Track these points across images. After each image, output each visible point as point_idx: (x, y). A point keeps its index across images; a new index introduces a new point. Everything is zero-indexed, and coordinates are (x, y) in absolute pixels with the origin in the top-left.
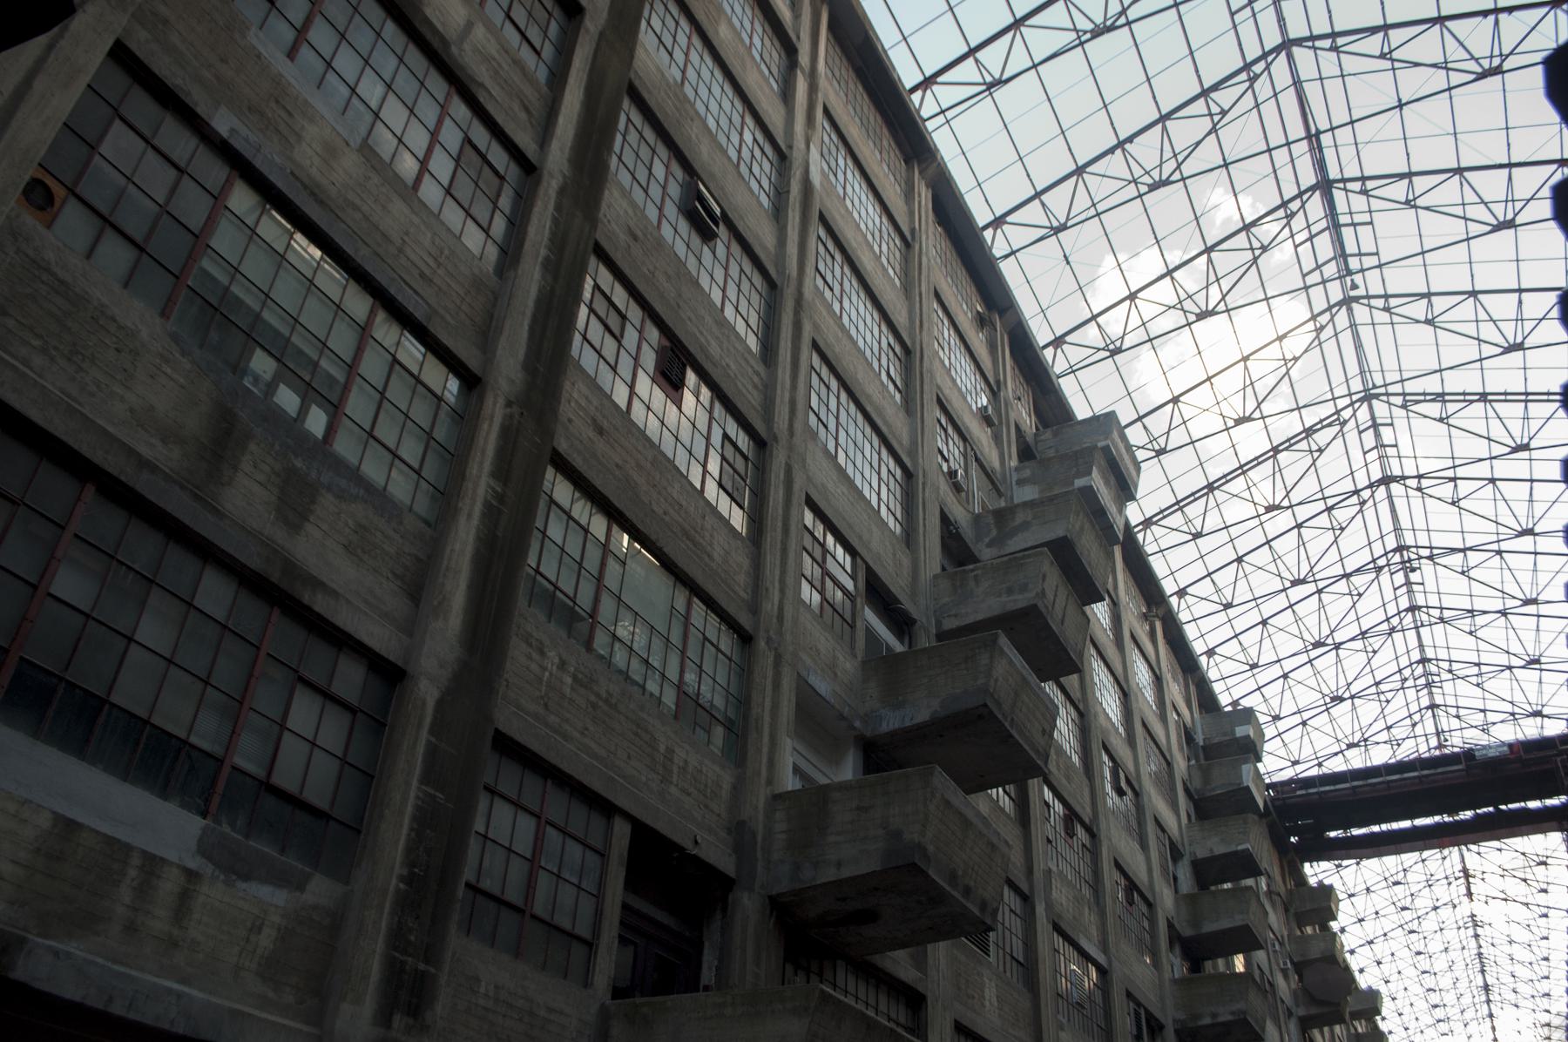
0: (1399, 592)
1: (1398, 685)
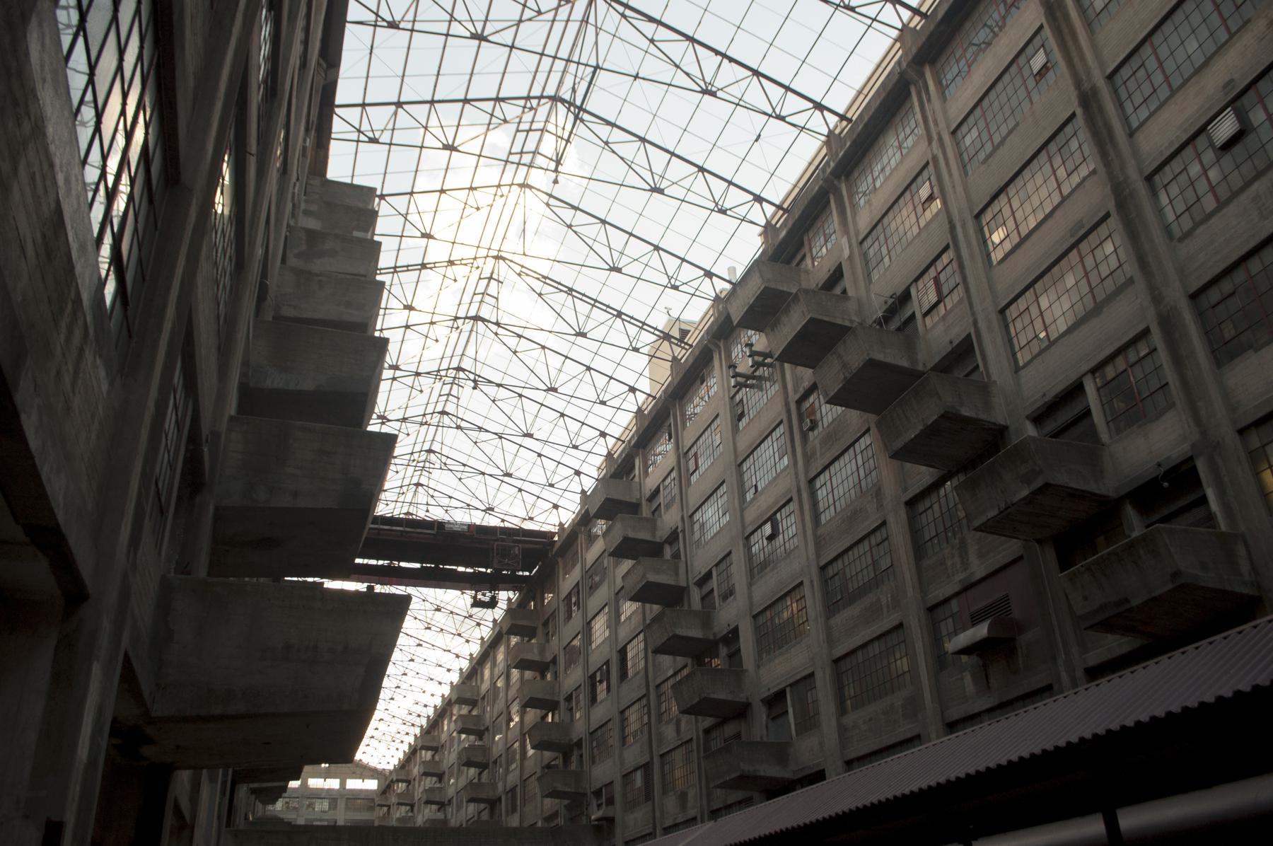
0: (441, 398)
1: (406, 462)
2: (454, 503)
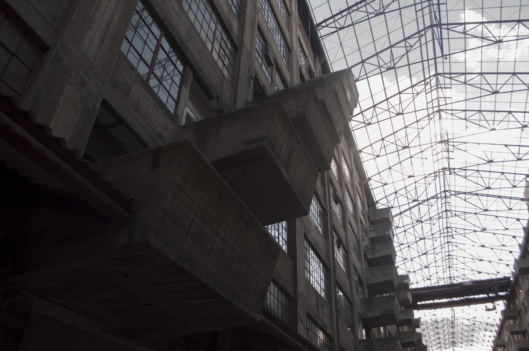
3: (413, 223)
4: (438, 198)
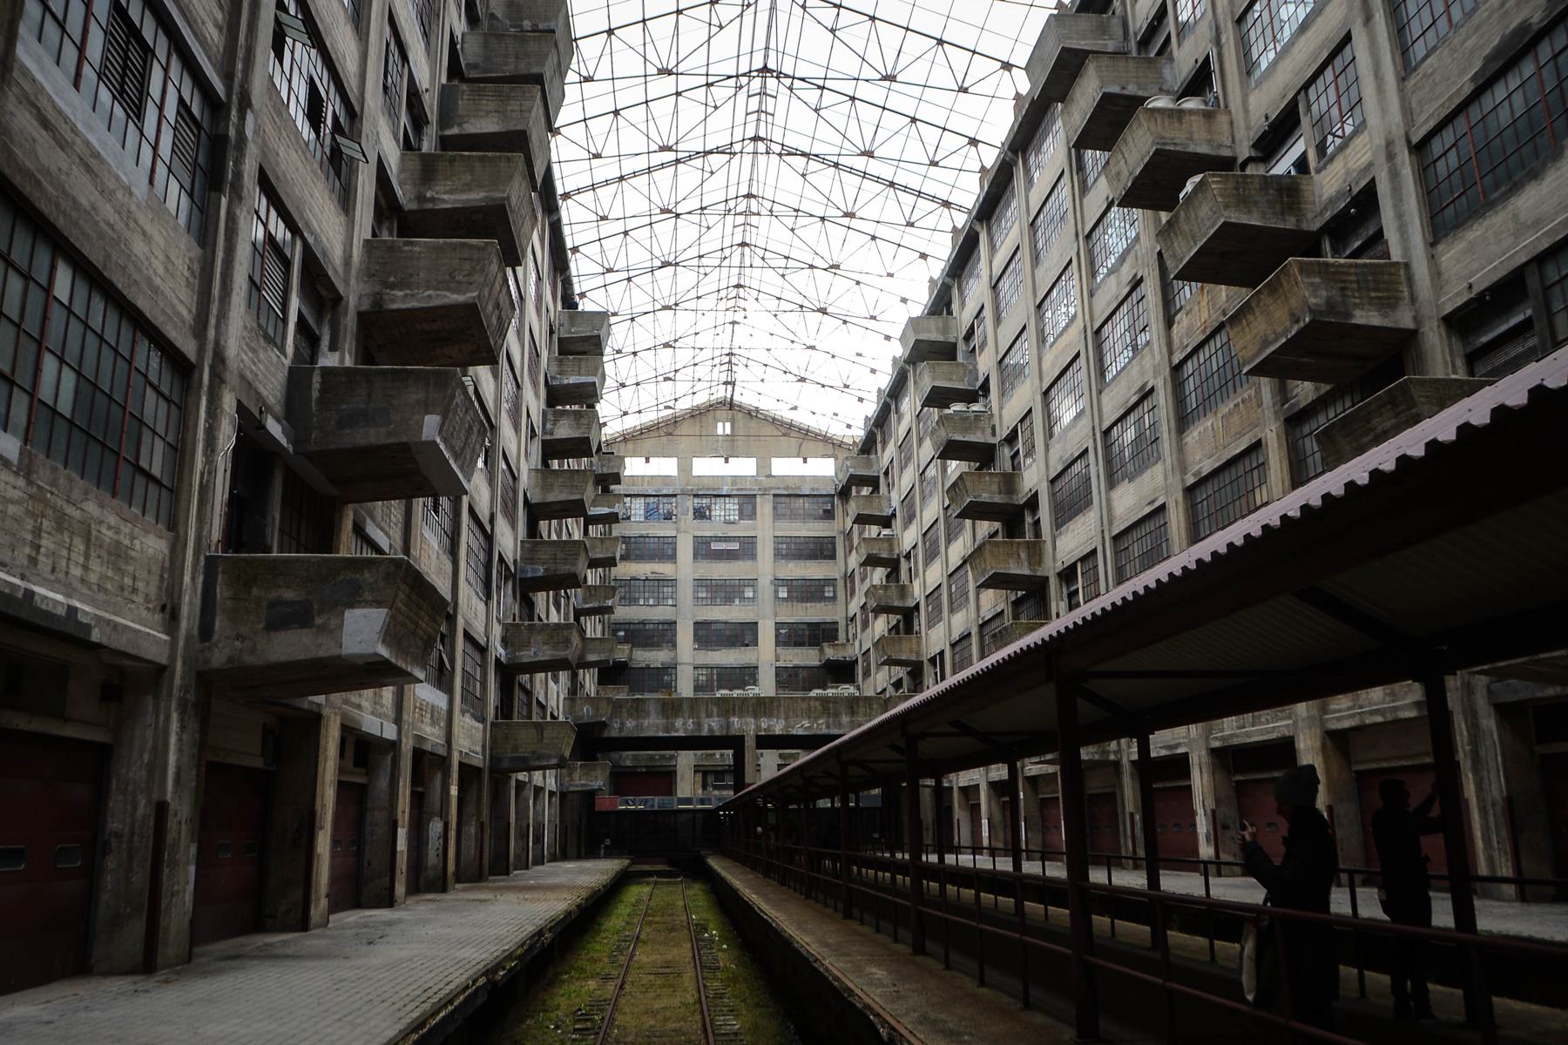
1: (717, 262)
2: (784, 305)
3: (652, 212)
4: (735, 154)
